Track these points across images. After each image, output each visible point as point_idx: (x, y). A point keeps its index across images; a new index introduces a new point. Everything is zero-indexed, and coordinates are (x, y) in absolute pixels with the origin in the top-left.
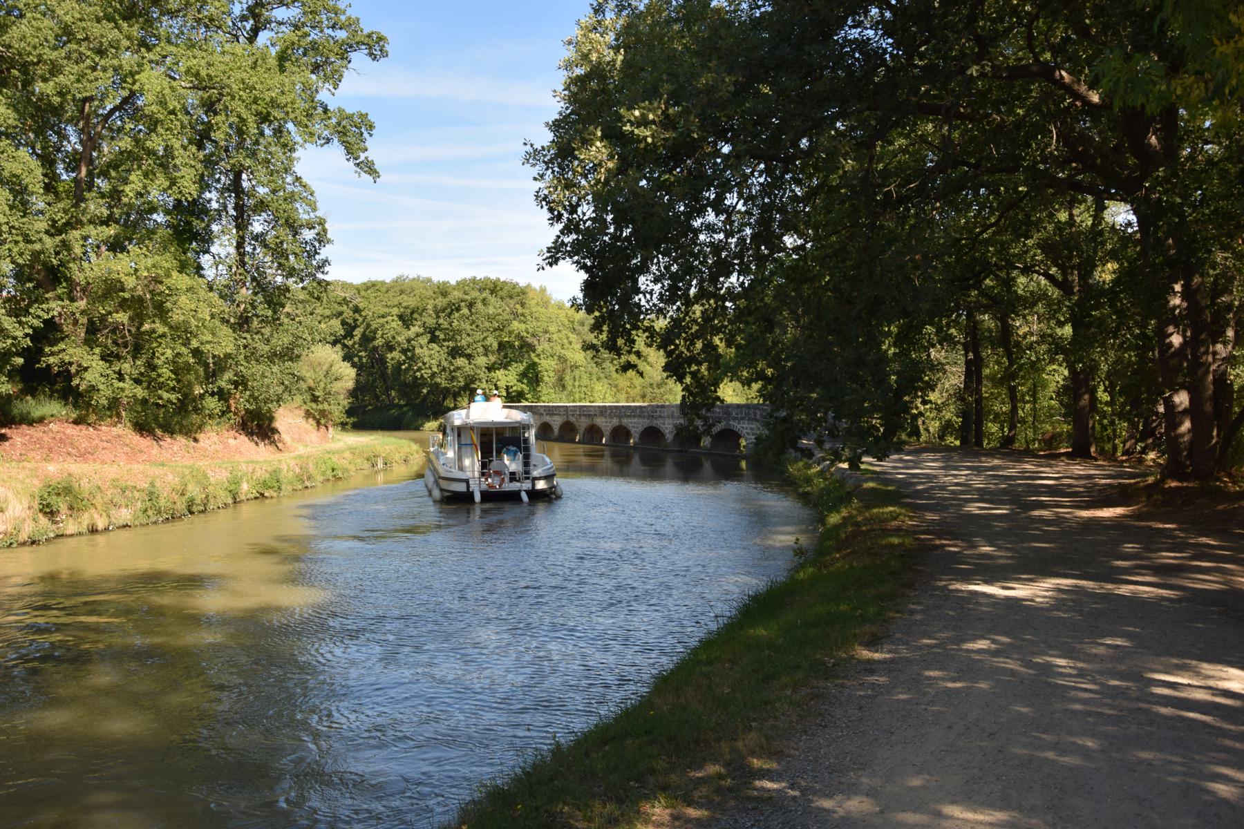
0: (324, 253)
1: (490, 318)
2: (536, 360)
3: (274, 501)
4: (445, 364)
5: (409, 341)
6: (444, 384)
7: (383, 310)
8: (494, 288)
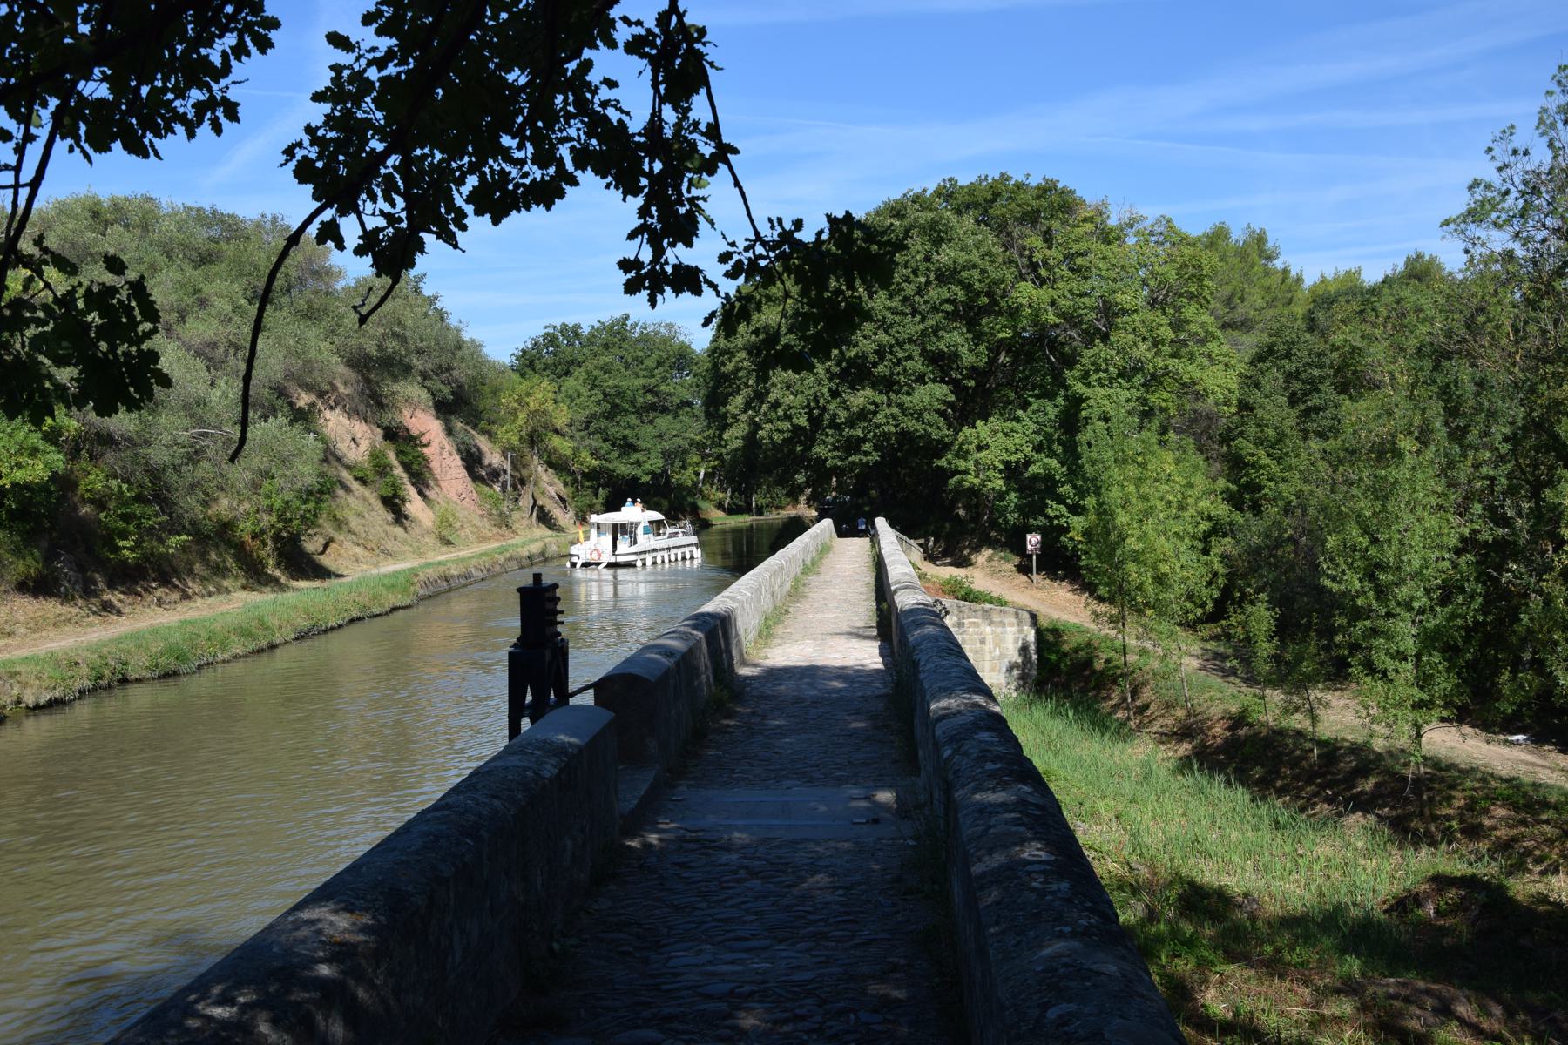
1: (945, 276)
2: (1079, 388)
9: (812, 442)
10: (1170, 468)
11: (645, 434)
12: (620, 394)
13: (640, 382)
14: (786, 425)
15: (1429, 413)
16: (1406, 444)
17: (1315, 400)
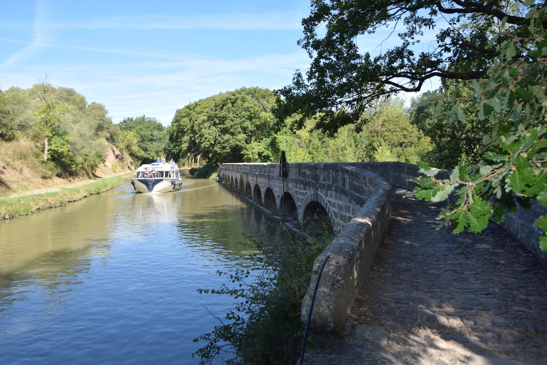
1: (247, 109)
6: (219, 151)
9: (213, 147)
10: (302, 152)
11: (149, 145)
12: (145, 136)
13: (149, 133)
14: (209, 143)
15: (352, 142)
16: (348, 147)
17: (324, 140)
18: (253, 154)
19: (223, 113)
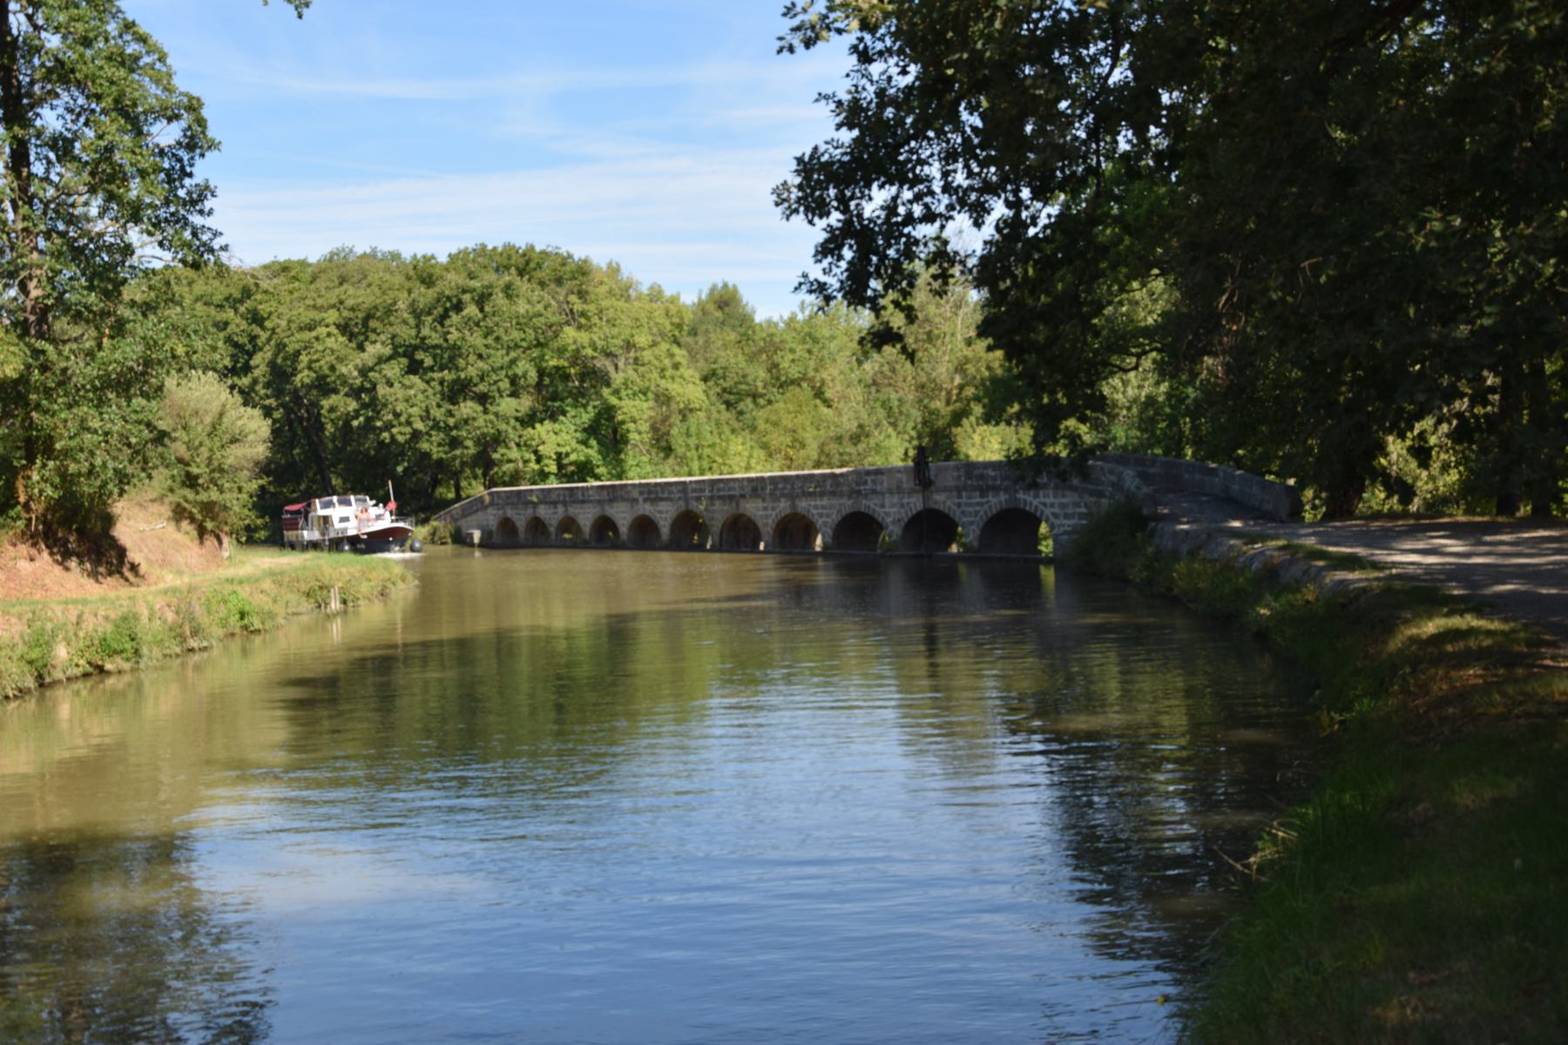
0: (203, 170)
2: (613, 401)
3: (127, 678)
4: (437, 413)
5: (364, 372)
6: (437, 453)
7: (309, 316)
8: (526, 264)
10: (740, 448)
14: (408, 430)
17: (741, 406)
18: (538, 461)
19: (454, 336)
